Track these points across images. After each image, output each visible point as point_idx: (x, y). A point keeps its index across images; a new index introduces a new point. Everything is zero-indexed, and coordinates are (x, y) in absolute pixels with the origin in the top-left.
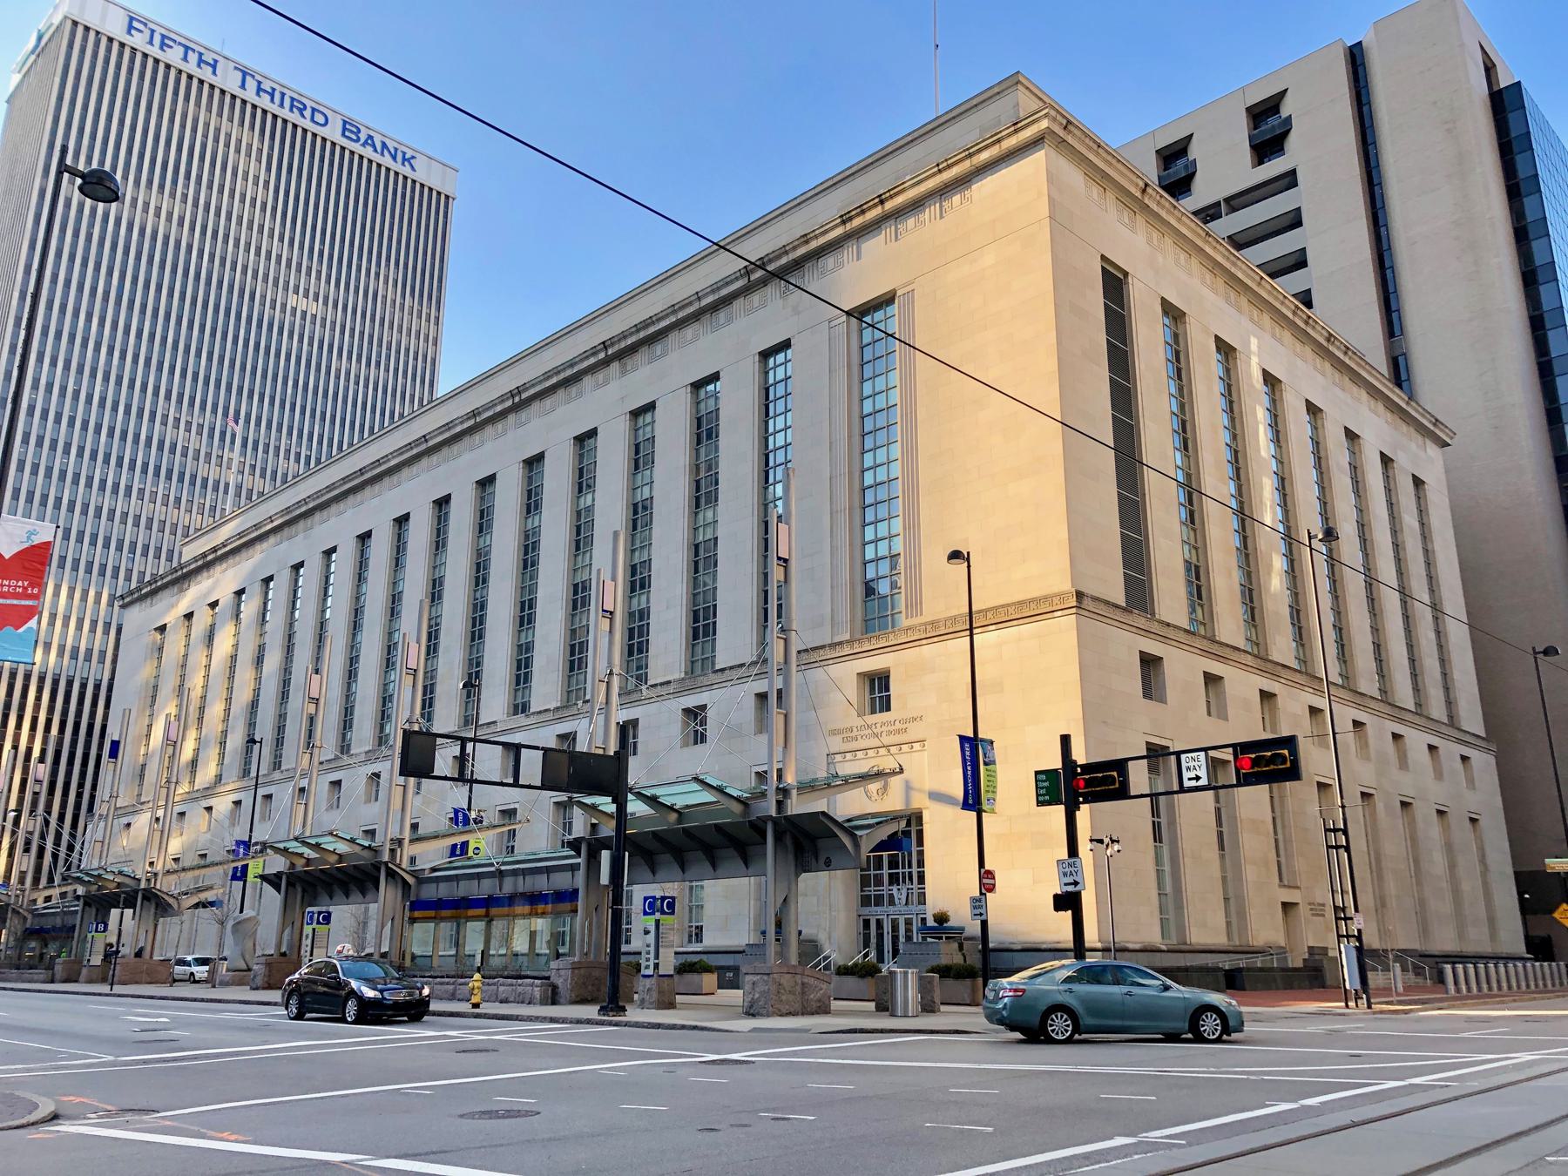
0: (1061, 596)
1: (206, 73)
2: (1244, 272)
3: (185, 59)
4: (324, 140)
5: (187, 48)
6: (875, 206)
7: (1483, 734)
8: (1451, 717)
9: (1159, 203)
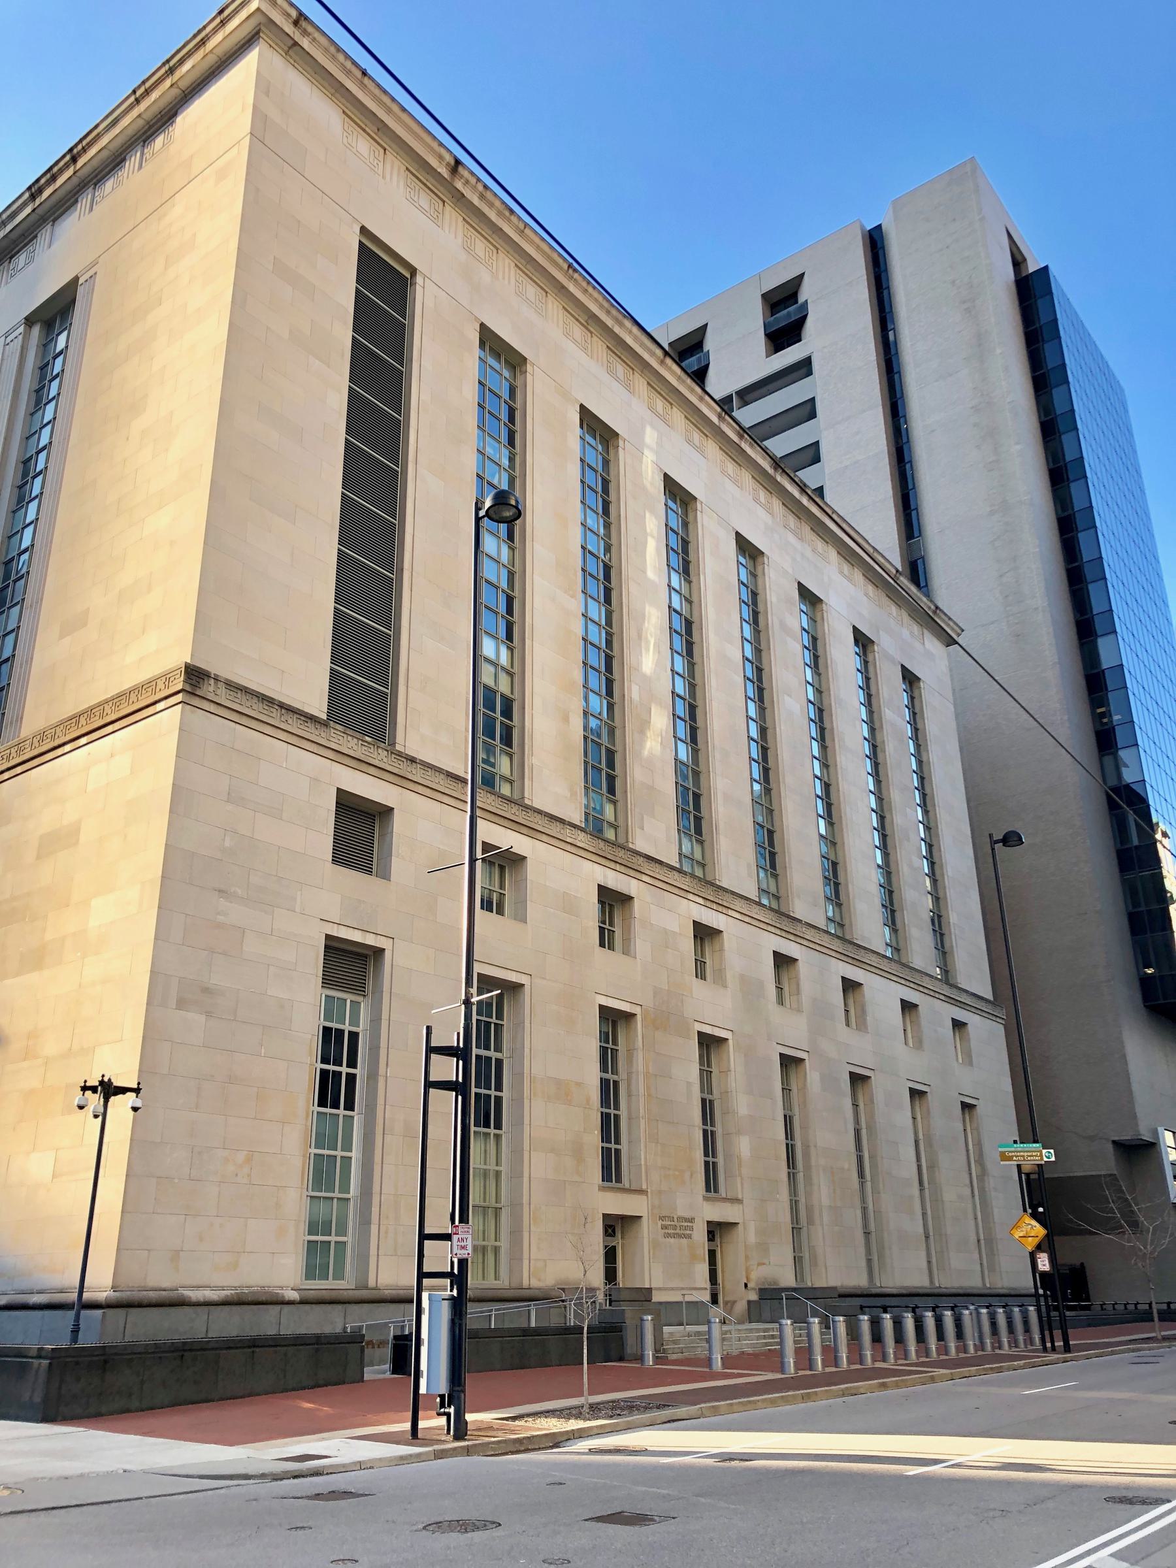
0: (167, 677)
6: (67, 166)
7: (989, 996)
8: (946, 972)
9: (482, 197)
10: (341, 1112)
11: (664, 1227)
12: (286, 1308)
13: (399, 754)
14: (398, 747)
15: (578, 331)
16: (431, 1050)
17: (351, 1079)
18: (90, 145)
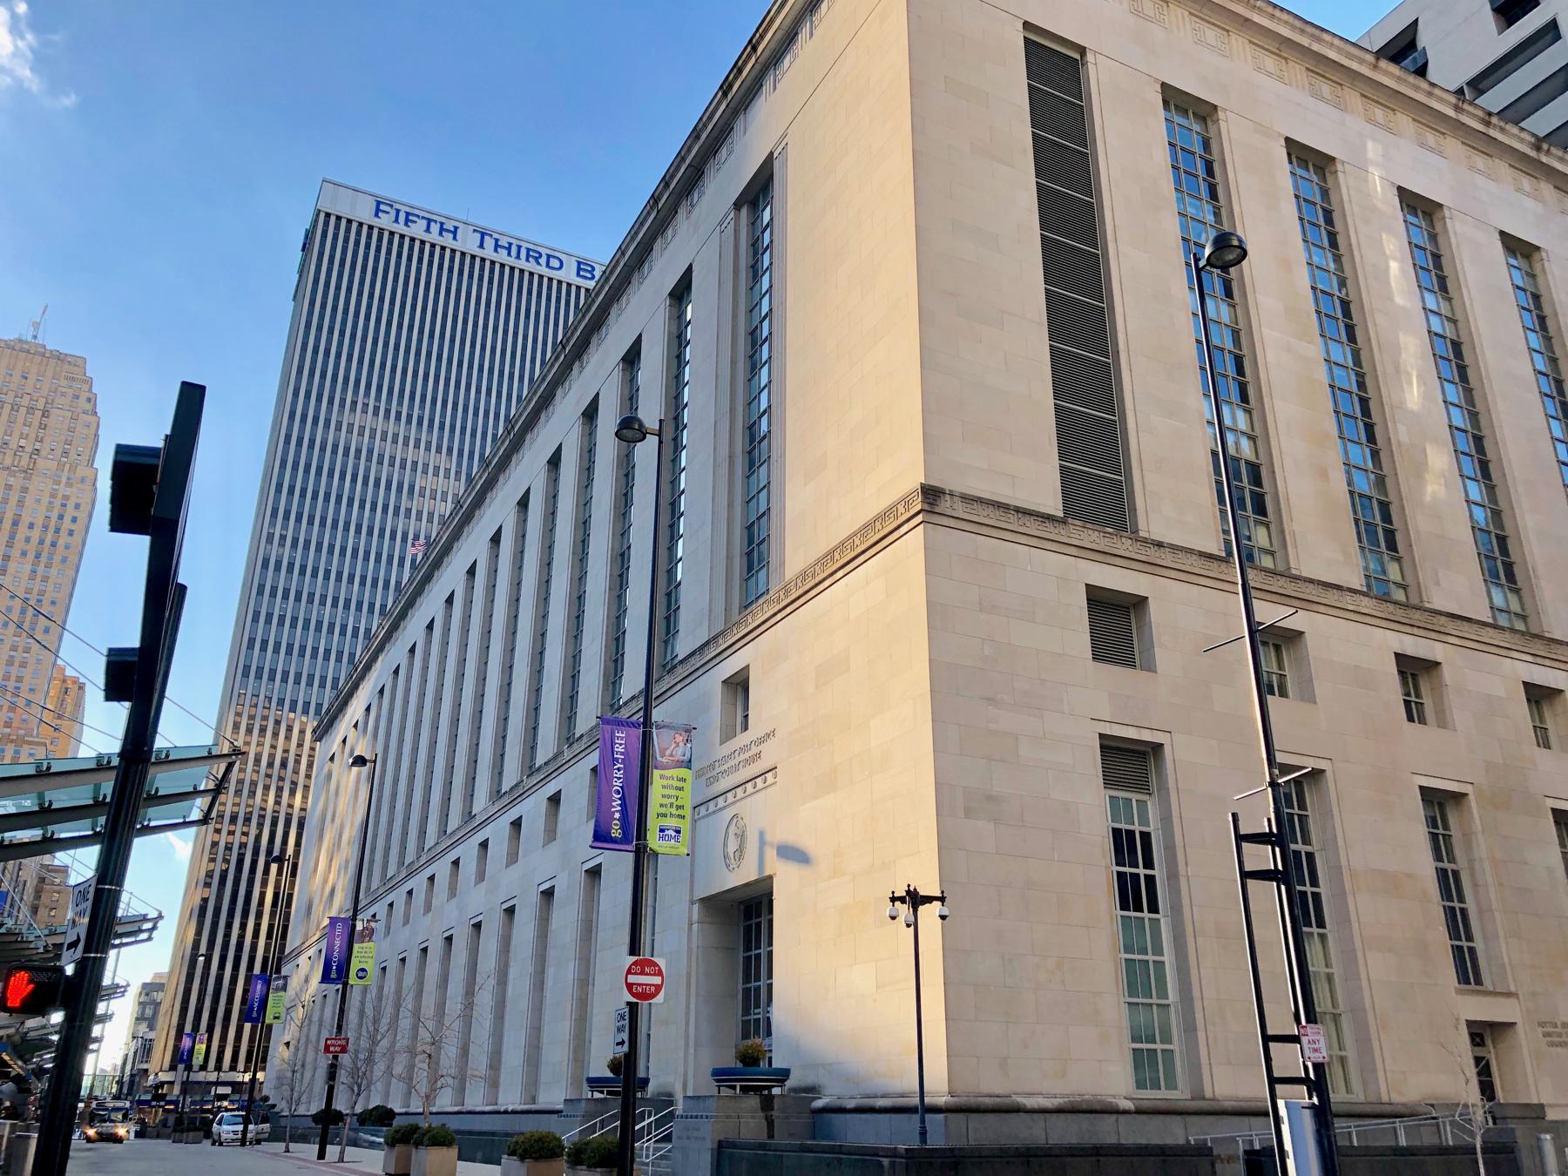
0: (906, 501)
1: (447, 240)
2: (1339, 50)
3: (428, 230)
4: (560, 282)
5: (429, 221)
6: (749, 57)
10: (1146, 914)
11: (1546, 1035)
12: (1122, 1118)
13: (1145, 541)
14: (1142, 534)
15: (1270, 62)
16: (1241, 838)
17: (1151, 880)
18: (766, 31)
